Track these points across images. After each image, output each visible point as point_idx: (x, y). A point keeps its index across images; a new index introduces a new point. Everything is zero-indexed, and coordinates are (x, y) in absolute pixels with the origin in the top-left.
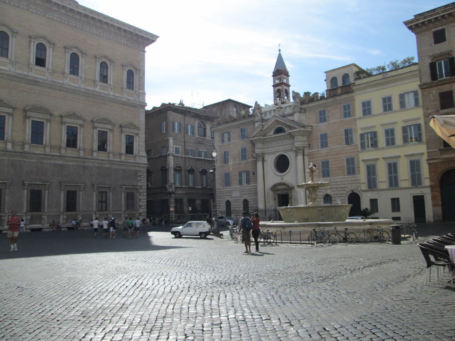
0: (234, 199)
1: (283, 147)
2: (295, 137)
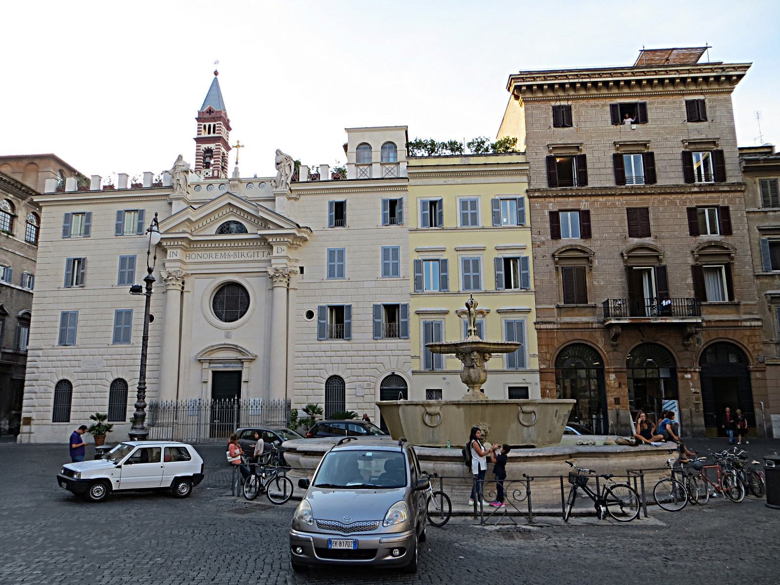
2: (275, 248)
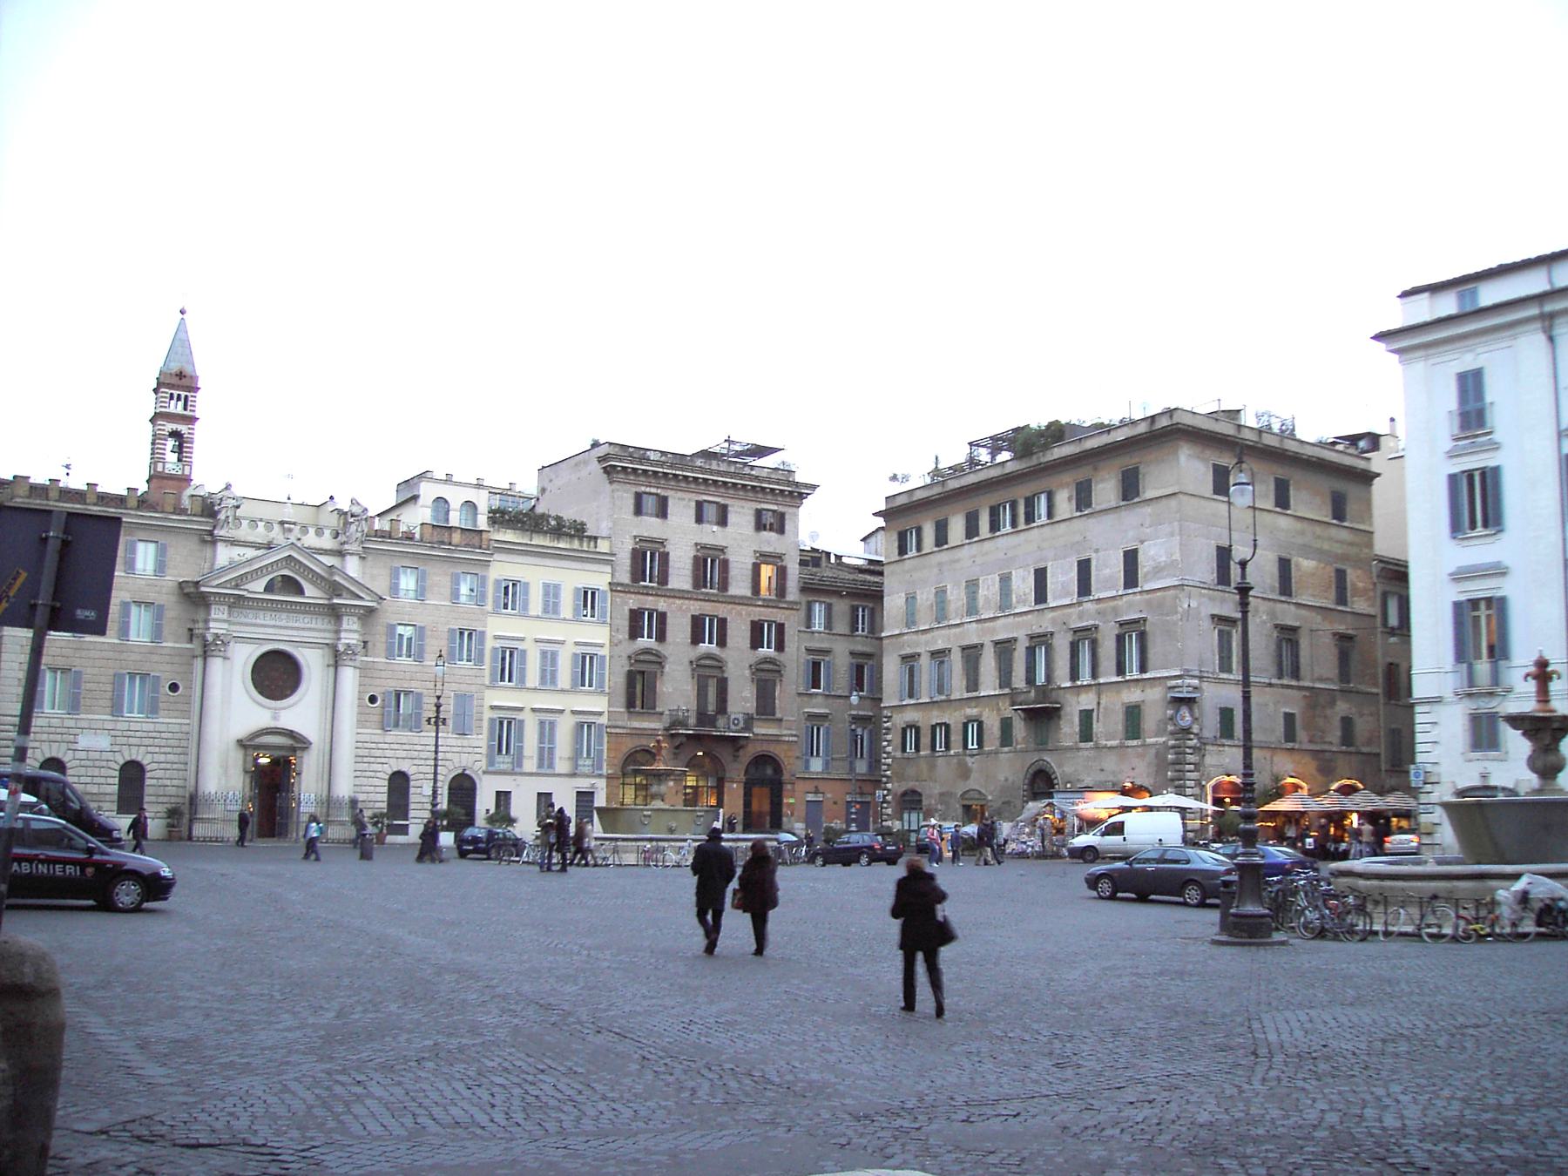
0: (83, 755)
1: (290, 632)
2: (345, 619)
